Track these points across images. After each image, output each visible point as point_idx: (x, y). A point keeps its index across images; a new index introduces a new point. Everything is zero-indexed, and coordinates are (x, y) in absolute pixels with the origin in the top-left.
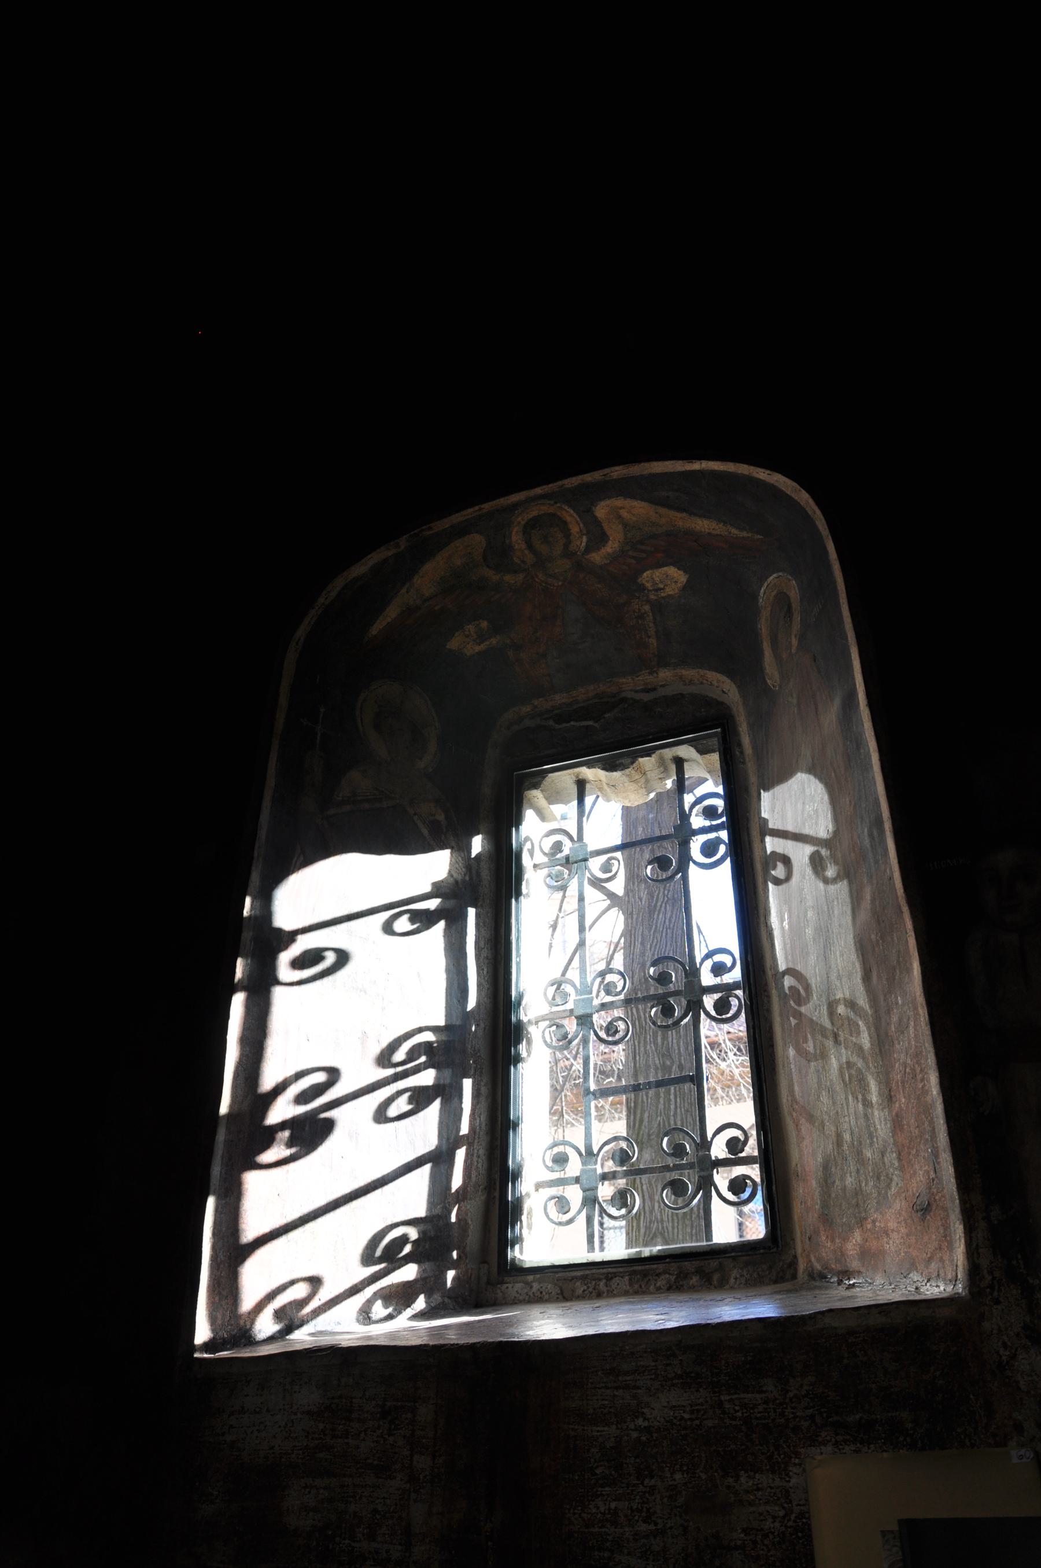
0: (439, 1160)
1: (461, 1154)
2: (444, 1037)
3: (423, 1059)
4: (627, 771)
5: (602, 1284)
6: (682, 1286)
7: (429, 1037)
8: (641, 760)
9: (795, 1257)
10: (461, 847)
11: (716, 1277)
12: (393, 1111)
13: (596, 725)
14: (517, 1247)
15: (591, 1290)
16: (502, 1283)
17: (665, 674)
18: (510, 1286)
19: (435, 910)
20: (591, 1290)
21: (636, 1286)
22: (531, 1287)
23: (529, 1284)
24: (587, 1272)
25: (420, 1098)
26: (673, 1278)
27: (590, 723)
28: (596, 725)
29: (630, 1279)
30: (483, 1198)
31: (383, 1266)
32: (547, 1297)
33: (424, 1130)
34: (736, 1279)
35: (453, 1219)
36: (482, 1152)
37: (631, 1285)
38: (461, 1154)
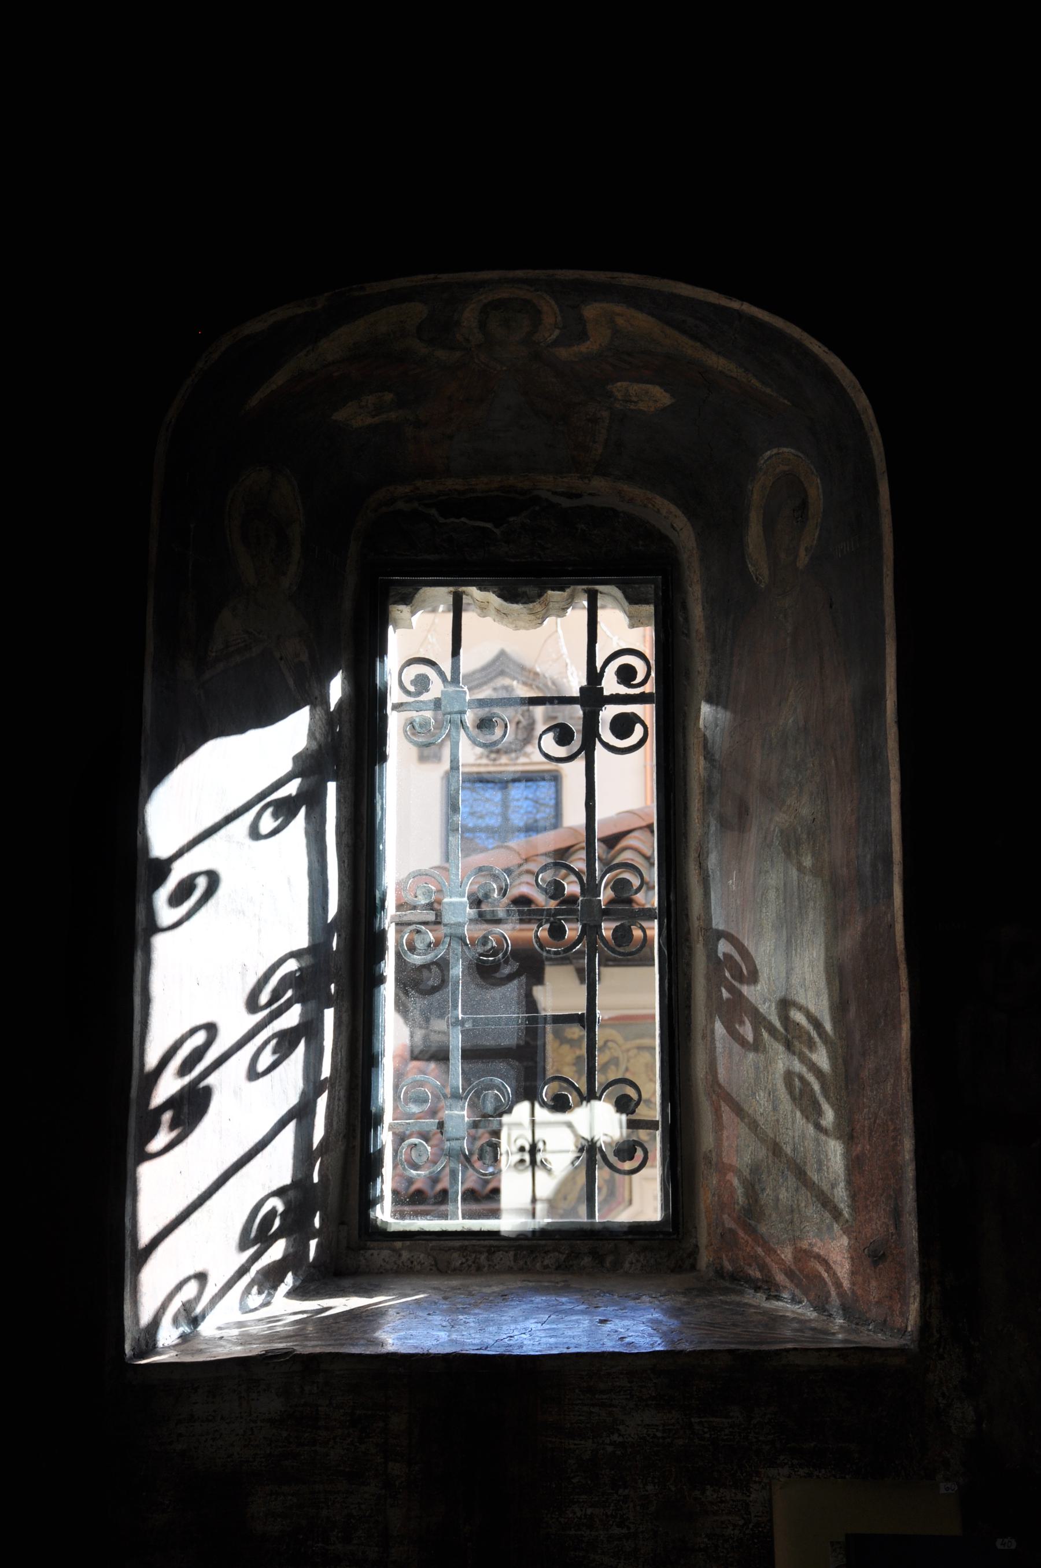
0: (301, 1113)
1: (322, 1102)
2: (307, 961)
3: (289, 993)
4: (531, 605)
5: (483, 1257)
6: (572, 1266)
7: (292, 965)
8: (550, 592)
9: (697, 1246)
10: (318, 700)
11: (609, 1260)
12: (261, 1067)
13: (497, 531)
14: (378, 1206)
15: (470, 1263)
16: (365, 1248)
17: (598, 483)
18: (375, 1252)
19: (297, 795)
20: (470, 1263)
21: (521, 1263)
22: (400, 1255)
23: (398, 1253)
24: (466, 1243)
25: (286, 1042)
26: (563, 1257)
27: (489, 525)
28: (497, 531)
29: (515, 1255)
30: (343, 1148)
31: (255, 1248)
32: (419, 1267)
33: (288, 1081)
34: (632, 1263)
35: (316, 1179)
36: (342, 1093)
37: (515, 1260)
38: (322, 1102)
